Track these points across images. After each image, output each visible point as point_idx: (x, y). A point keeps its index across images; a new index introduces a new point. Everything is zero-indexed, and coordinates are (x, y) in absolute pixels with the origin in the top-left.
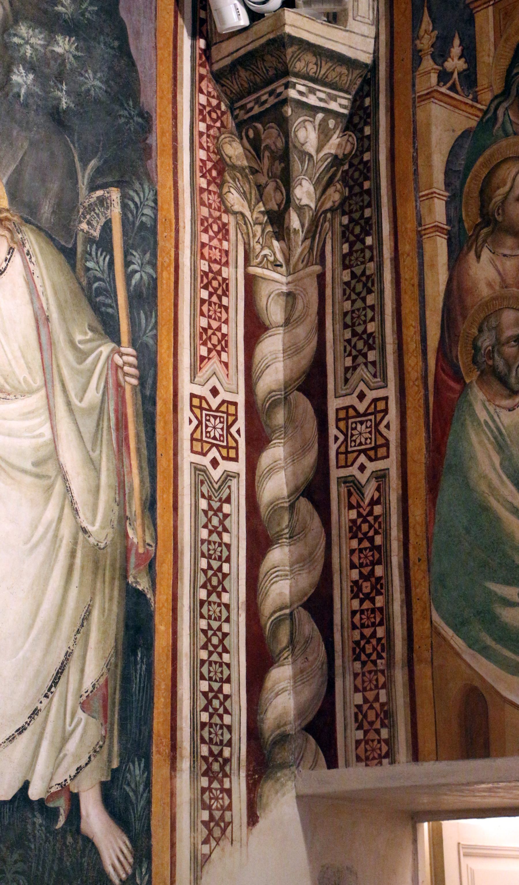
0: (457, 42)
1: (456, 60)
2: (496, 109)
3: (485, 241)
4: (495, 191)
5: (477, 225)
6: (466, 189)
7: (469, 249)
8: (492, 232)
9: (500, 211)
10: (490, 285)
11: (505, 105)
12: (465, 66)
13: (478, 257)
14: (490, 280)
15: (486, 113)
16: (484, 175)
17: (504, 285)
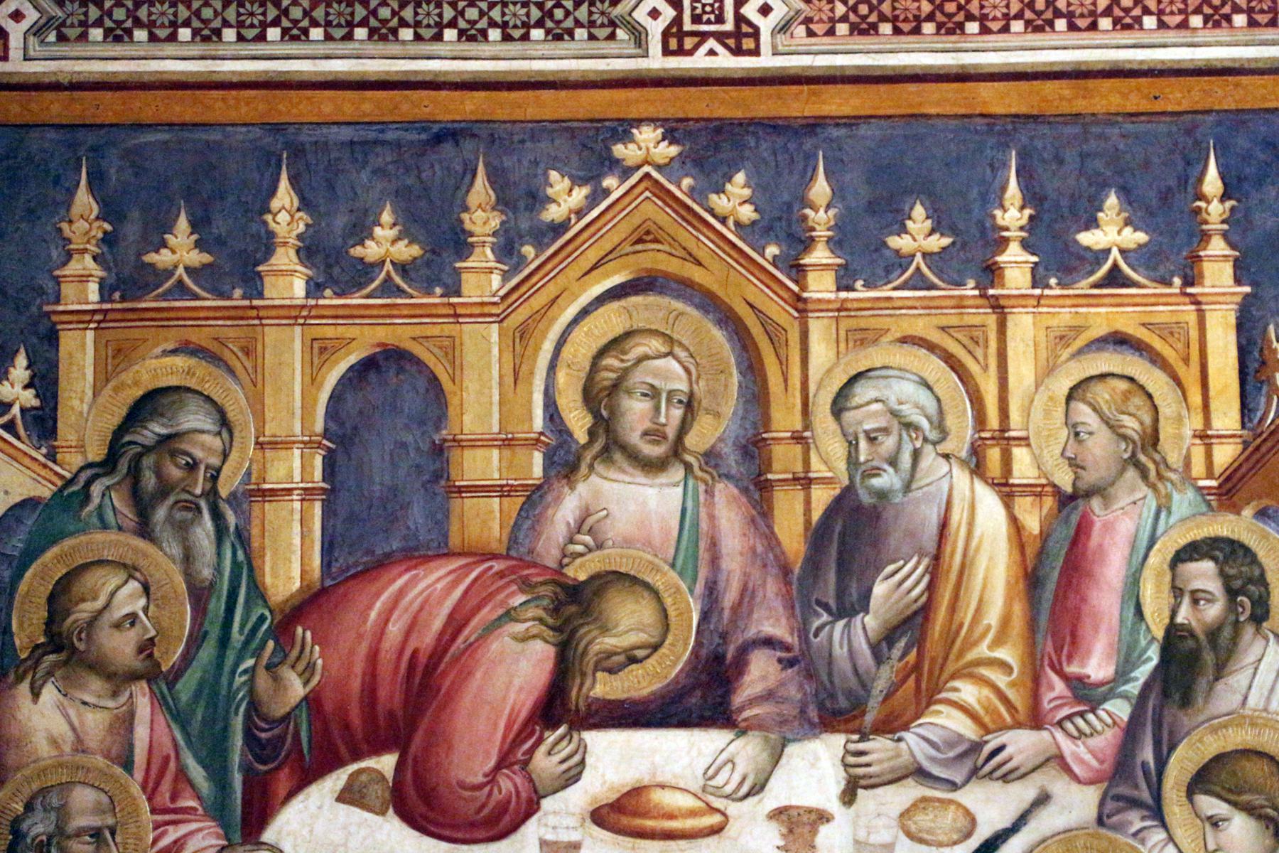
0: (21, 360)
1: (18, 388)
2: (88, 484)
3: (50, 674)
4: (77, 604)
5: (37, 646)
6: (23, 587)
7: (20, 679)
8: (66, 663)
9: (83, 636)
10: (54, 742)
11: (107, 481)
12: (36, 403)
13: (36, 694)
14: (56, 735)
15: (70, 482)
16: (60, 575)
17: (80, 746)
